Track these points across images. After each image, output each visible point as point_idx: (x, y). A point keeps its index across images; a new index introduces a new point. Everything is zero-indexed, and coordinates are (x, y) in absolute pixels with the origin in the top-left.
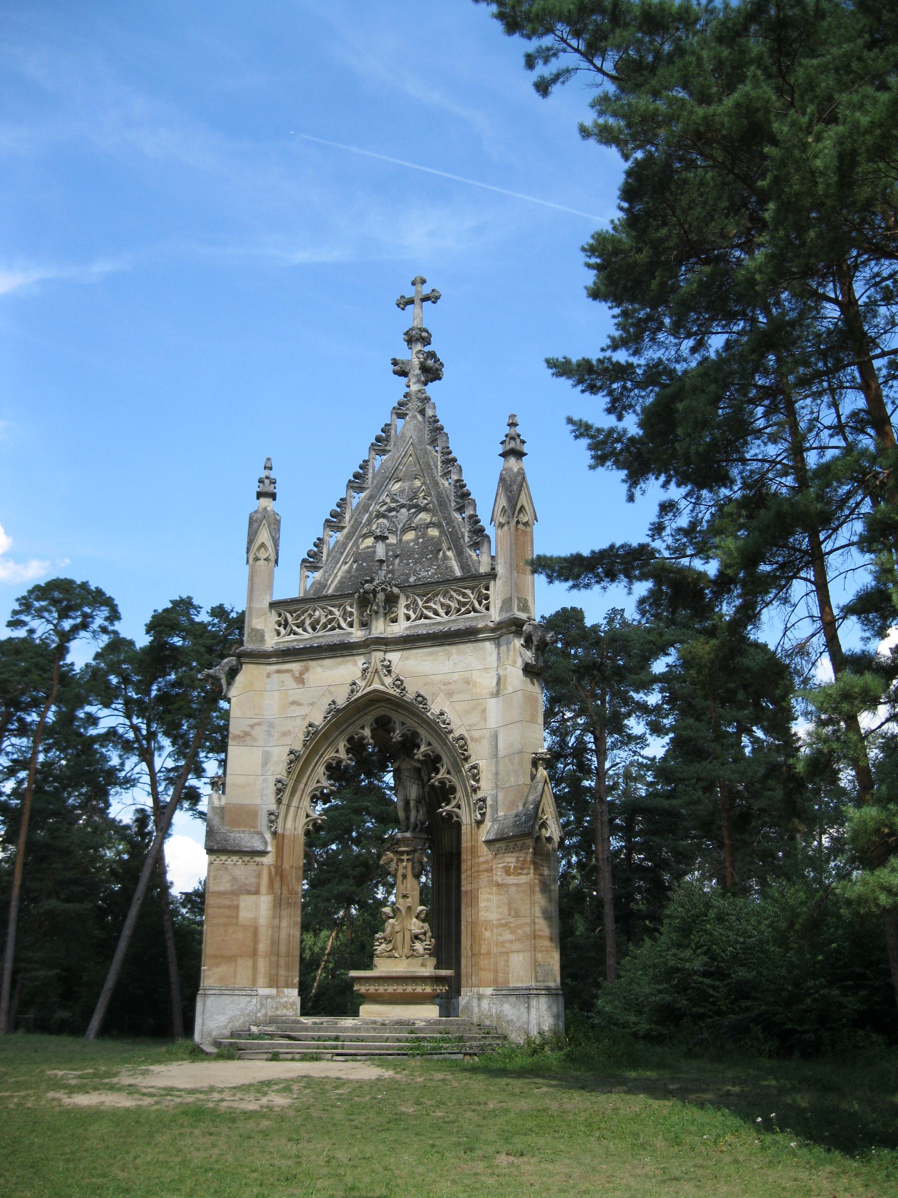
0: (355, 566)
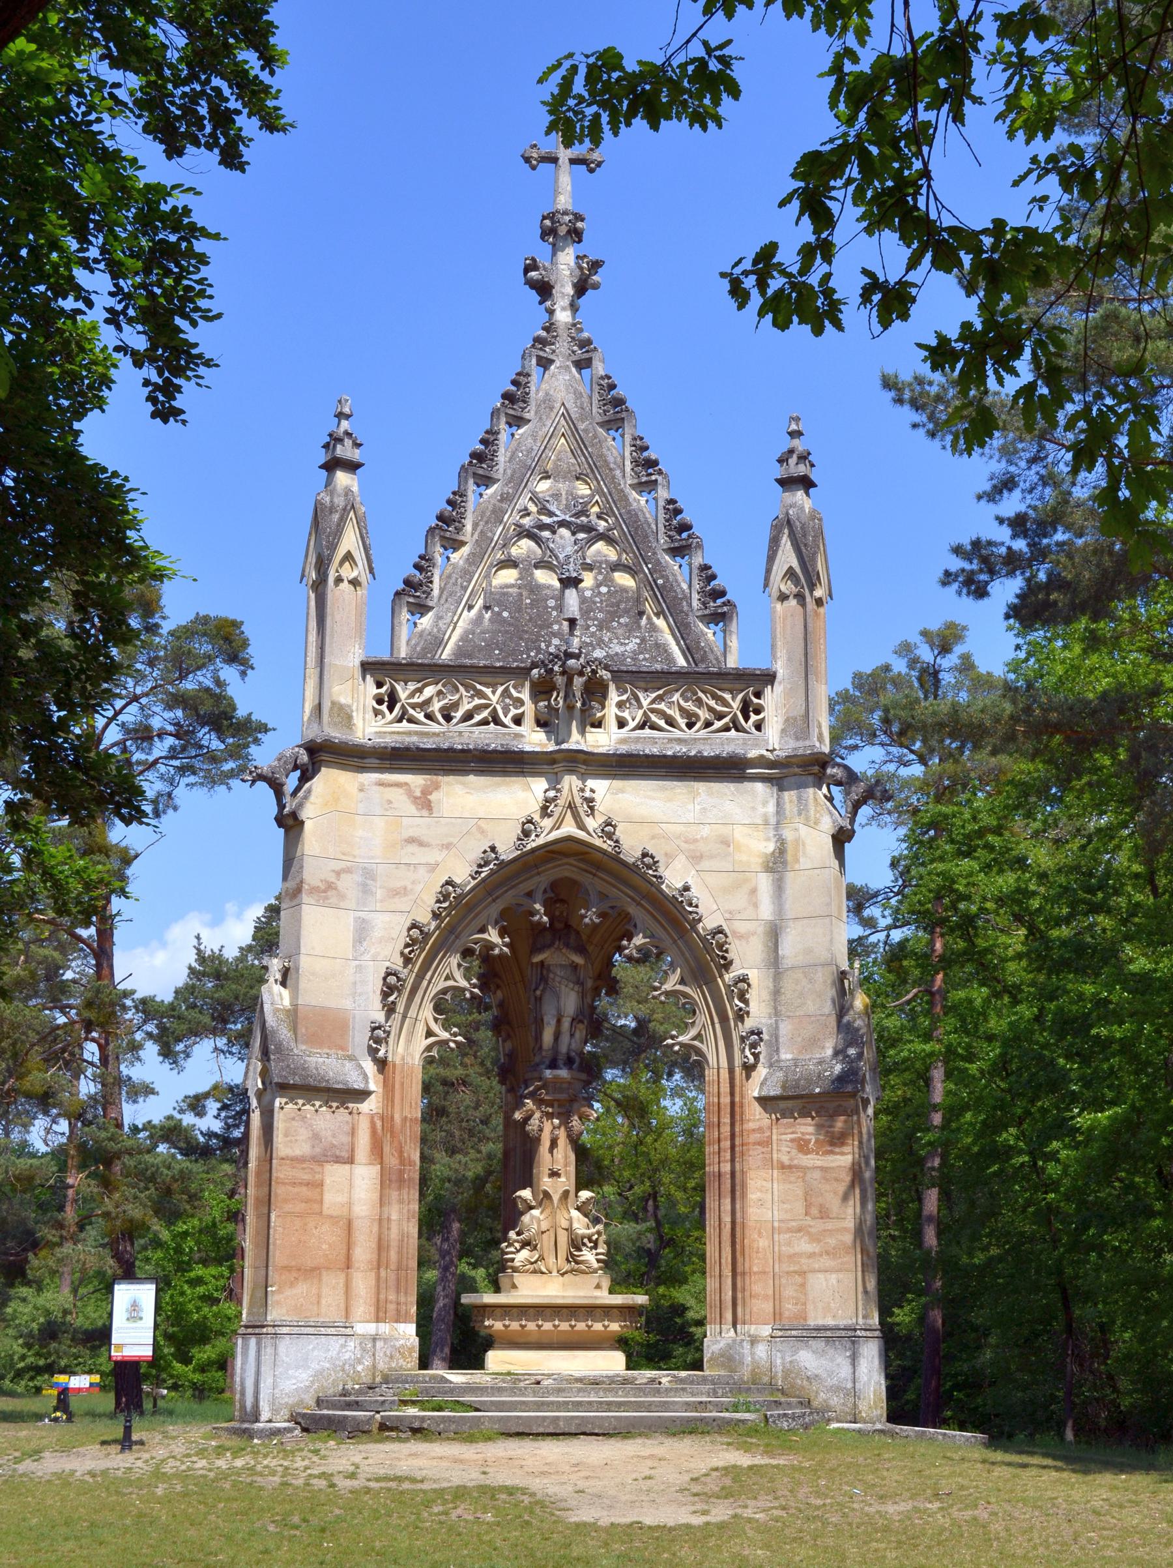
0: (488, 615)
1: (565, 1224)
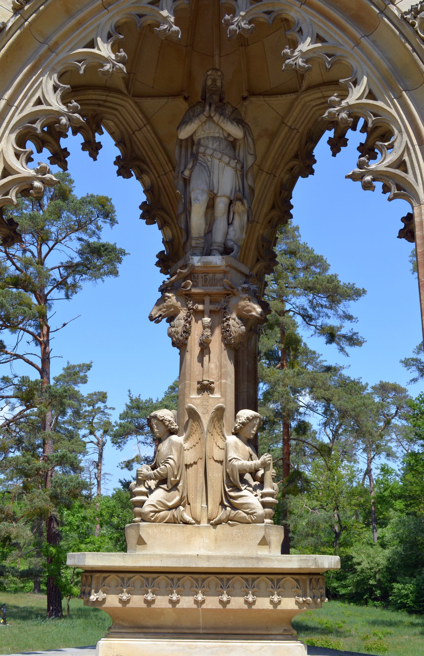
1: (218, 454)
